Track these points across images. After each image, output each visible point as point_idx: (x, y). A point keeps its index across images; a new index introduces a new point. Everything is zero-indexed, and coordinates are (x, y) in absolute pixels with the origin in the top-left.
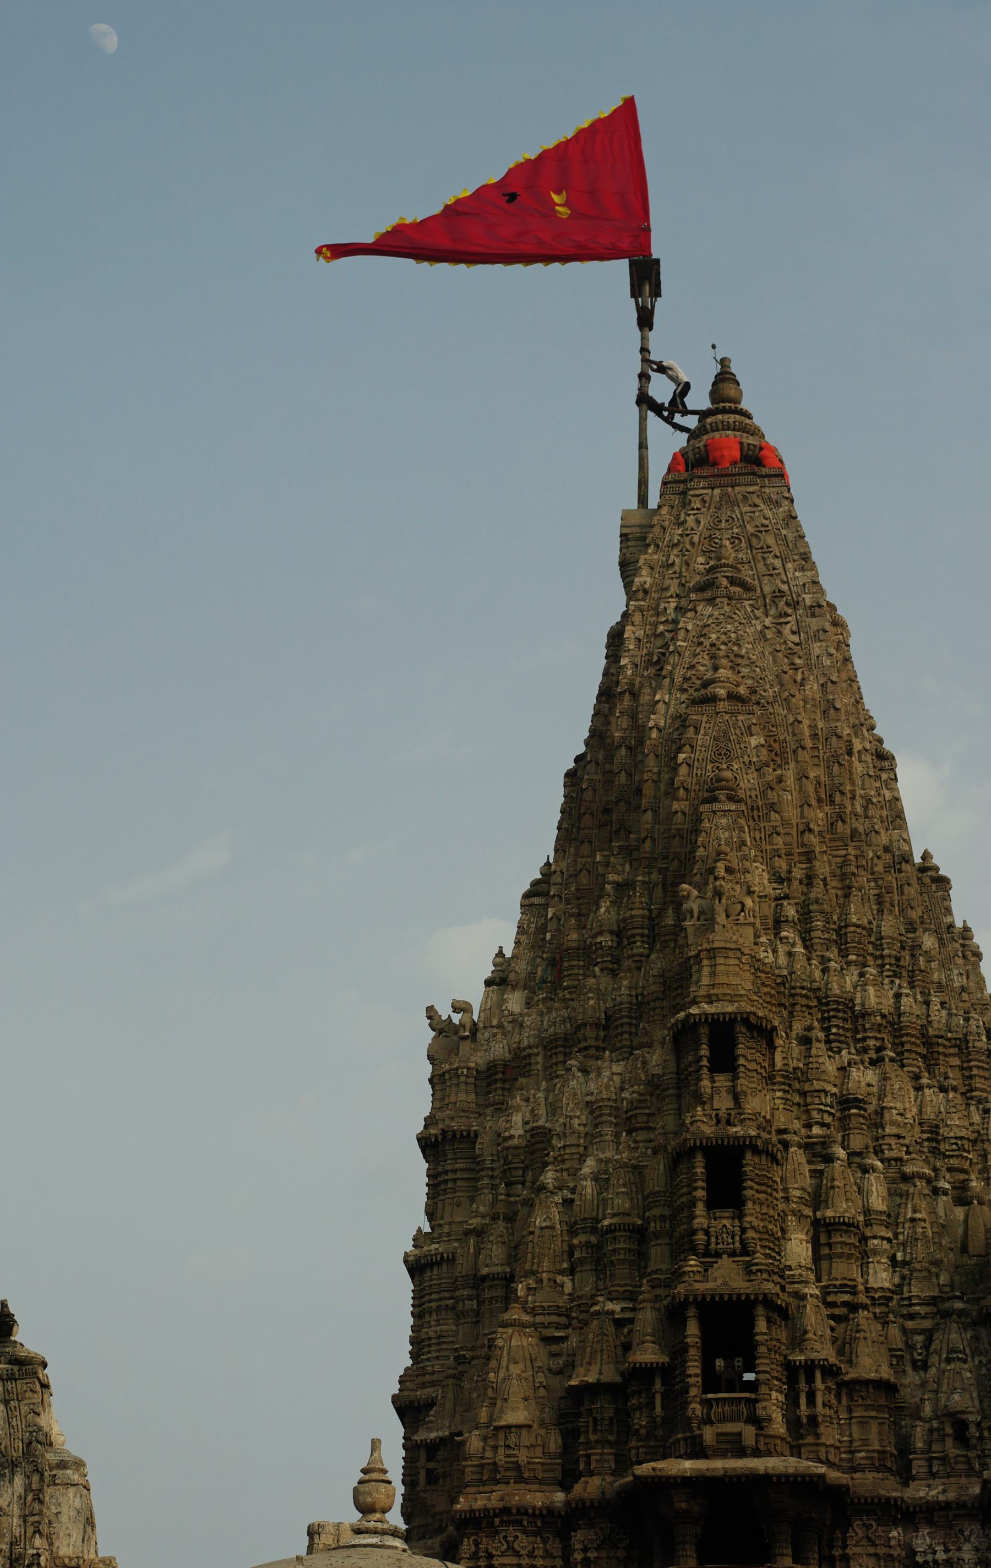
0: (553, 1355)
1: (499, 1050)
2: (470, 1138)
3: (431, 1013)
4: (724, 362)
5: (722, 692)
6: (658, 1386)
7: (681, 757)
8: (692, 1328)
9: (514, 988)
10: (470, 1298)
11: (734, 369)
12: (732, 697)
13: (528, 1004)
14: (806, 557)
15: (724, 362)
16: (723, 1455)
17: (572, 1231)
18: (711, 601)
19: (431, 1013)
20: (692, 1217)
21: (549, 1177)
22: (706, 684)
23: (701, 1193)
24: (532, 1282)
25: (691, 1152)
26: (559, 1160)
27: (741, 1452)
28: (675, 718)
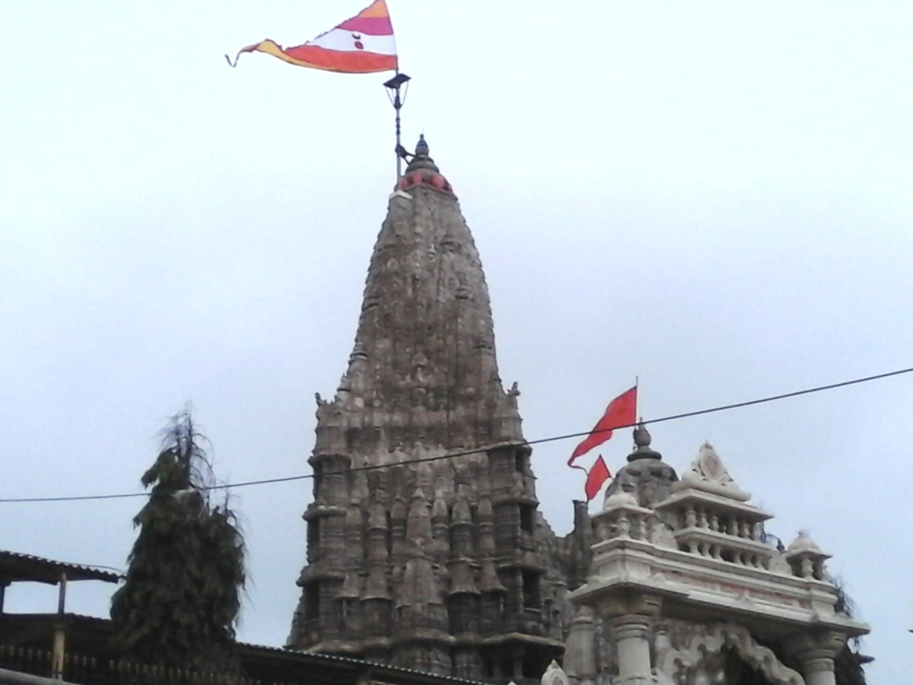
0: (435, 574)
1: (356, 422)
2: (348, 462)
3: (318, 396)
4: (422, 136)
5: (471, 296)
6: (502, 600)
7: (460, 320)
8: (520, 579)
9: (359, 395)
10: (358, 535)
11: (426, 139)
12: (473, 300)
13: (369, 404)
14: (473, 241)
15: (422, 136)
16: (531, 634)
17: (433, 521)
18: (451, 251)
19: (318, 396)
20: (516, 531)
21: (419, 492)
22: (460, 290)
23: (519, 522)
24: (422, 539)
25: (512, 503)
26: (423, 487)
27: (538, 634)
28: (449, 300)
